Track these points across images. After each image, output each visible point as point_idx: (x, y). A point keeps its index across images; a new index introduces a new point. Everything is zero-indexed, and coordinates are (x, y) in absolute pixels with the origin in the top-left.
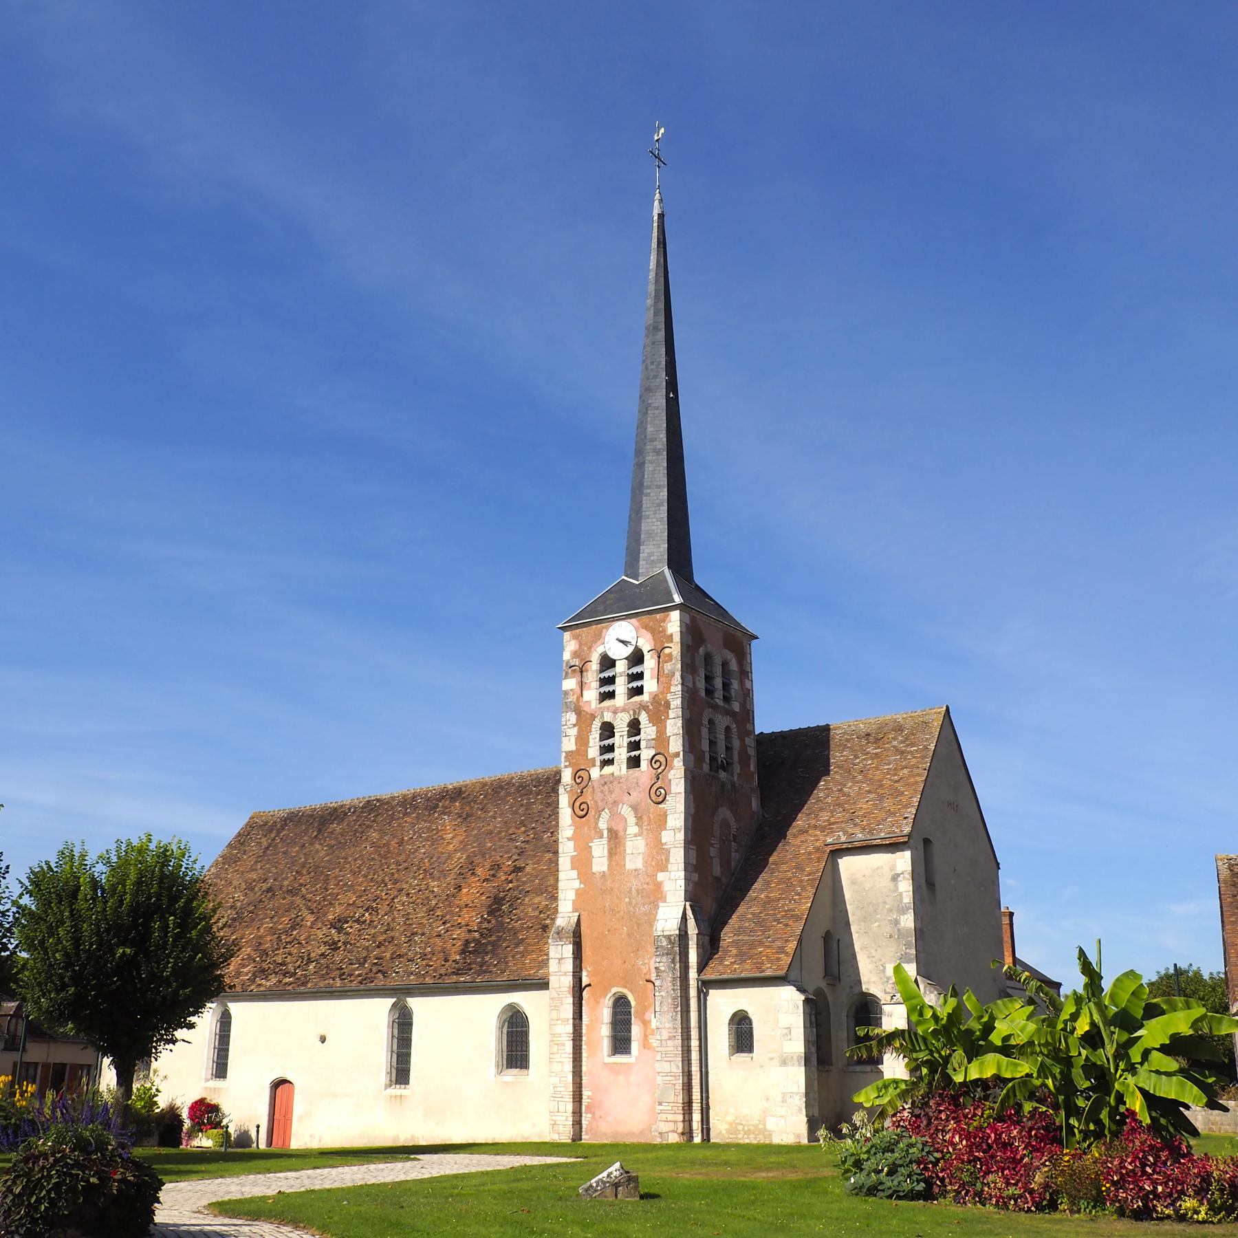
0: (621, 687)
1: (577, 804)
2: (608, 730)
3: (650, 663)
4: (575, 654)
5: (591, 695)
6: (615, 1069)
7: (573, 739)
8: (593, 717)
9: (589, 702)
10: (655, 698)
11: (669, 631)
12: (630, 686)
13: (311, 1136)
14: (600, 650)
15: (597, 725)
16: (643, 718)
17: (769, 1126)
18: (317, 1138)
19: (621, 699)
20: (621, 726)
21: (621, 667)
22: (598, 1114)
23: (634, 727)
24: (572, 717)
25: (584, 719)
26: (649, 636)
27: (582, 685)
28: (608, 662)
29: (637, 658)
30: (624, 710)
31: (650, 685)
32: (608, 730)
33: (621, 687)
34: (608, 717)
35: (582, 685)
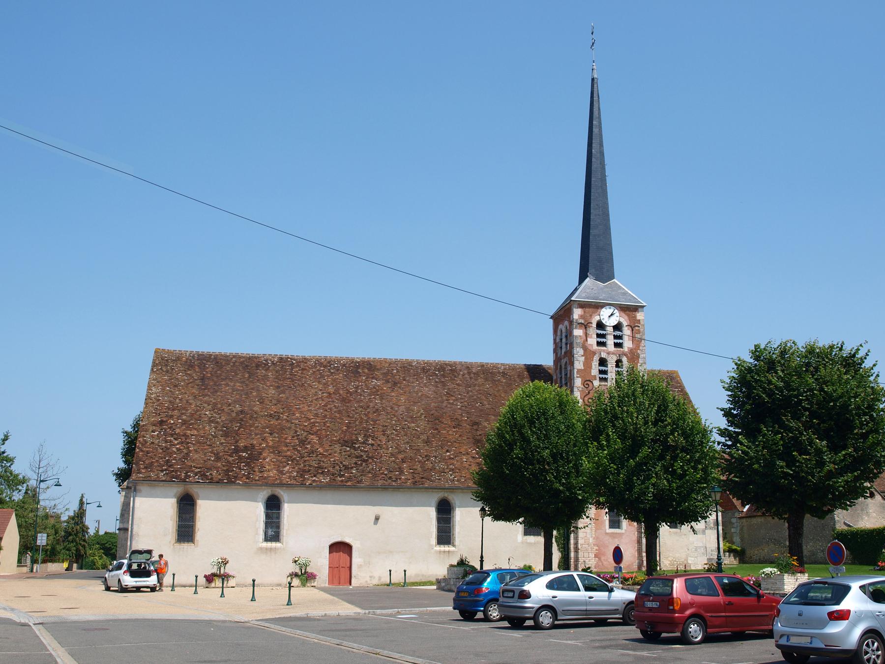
0: (610, 341)
1: (586, 399)
2: (603, 362)
3: (627, 331)
4: (581, 317)
5: (592, 341)
6: (613, 535)
7: (582, 363)
8: (594, 353)
9: (592, 345)
10: (631, 350)
11: (638, 318)
12: (621, 341)
13: (371, 577)
14: (597, 318)
15: (596, 359)
16: (624, 359)
17: (690, 562)
18: (377, 578)
19: (611, 347)
20: (612, 361)
21: (610, 330)
22: (603, 558)
23: (618, 363)
24: (581, 352)
25: (589, 354)
26: (626, 317)
27: (586, 335)
28: (600, 326)
29: (618, 327)
30: (613, 354)
31: (628, 344)
32: (603, 362)
33: (610, 341)
34: (604, 355)
35: (586, 335)
